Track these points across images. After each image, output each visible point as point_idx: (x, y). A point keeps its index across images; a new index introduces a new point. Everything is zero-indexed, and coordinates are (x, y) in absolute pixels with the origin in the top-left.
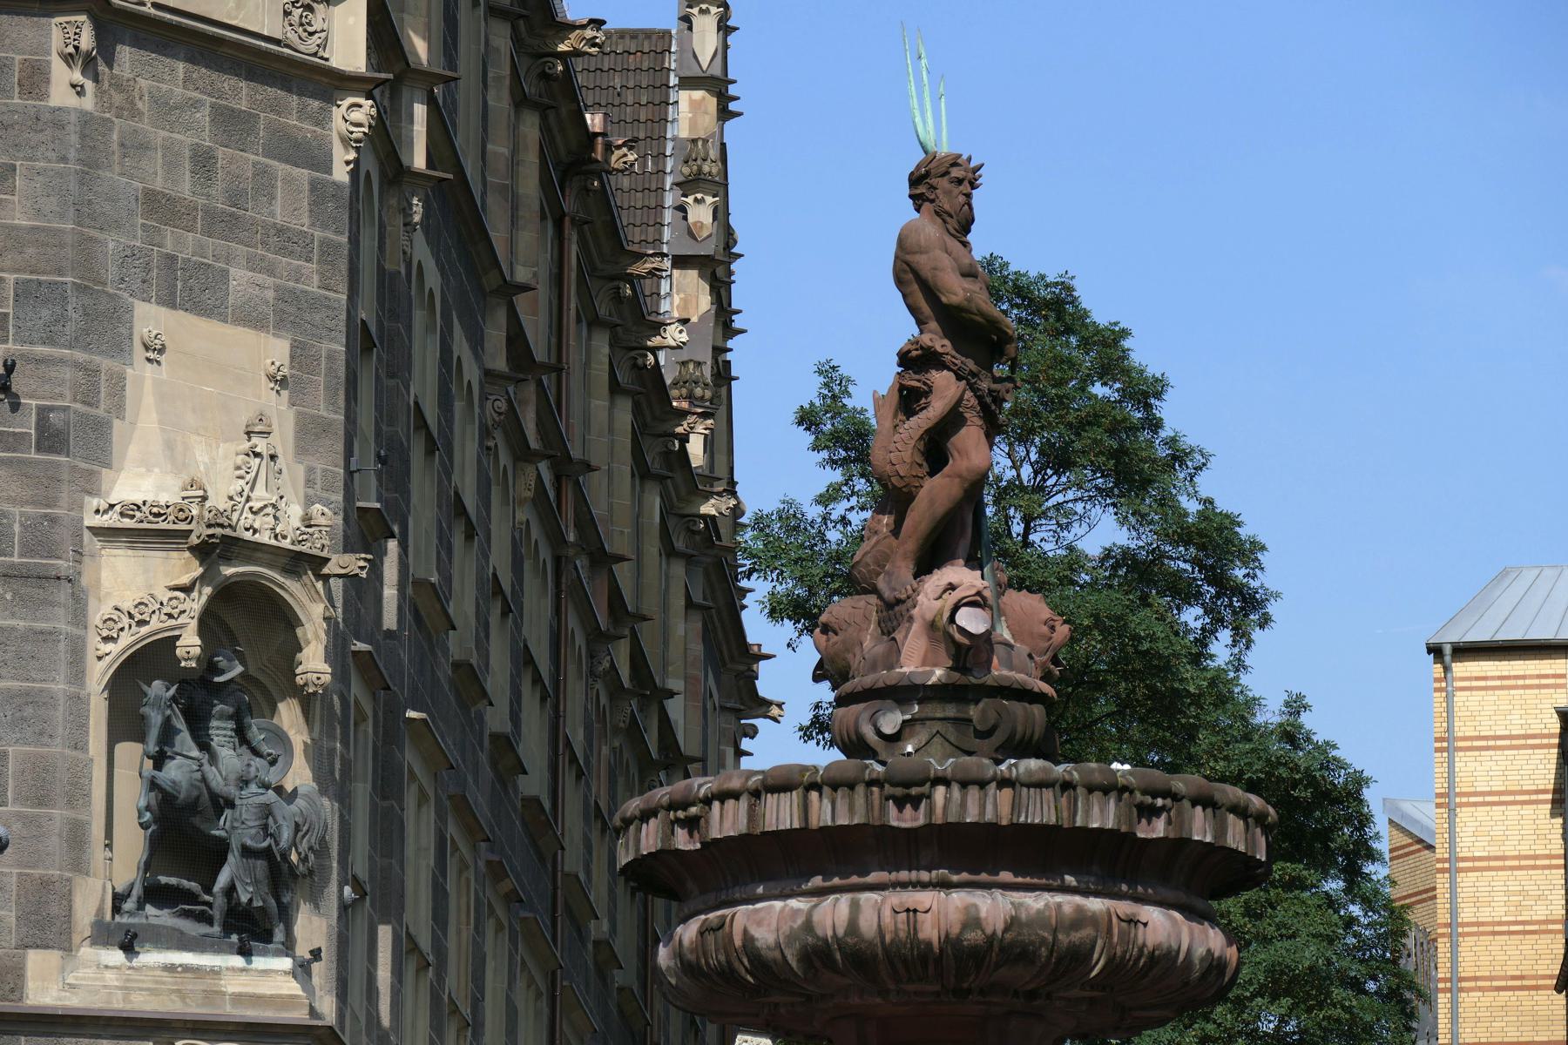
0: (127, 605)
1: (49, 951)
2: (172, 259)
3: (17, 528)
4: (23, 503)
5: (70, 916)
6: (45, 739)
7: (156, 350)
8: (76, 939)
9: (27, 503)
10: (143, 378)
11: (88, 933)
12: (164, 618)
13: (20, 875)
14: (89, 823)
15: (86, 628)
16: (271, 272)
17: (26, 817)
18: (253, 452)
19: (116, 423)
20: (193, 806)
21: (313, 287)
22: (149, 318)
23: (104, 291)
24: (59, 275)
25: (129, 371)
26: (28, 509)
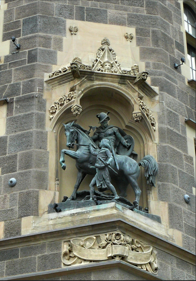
0: (57, 101)
1: (29, 217)
2: (82, 8)
3: (21, 87)
4: (24, 79)
5: (38, 204)
6: (29, 147)
7: (73, 31)
8: (40, 212)
9: (25, 78)
10: (67, 39)
11: (46, 210)
12: (68, 101)
13: (20, 193)
14: (47, 172)
15: (45, 111)
16: (125, 10)
17: (22, 173)
18: (102, 49)
19: (59, 53)
20: (87, 160)
21: (145, 13)
22: (70, 23)
23: (52, 17)
24: (35, 14)
25: (64, 38)
26: (26, 80)
